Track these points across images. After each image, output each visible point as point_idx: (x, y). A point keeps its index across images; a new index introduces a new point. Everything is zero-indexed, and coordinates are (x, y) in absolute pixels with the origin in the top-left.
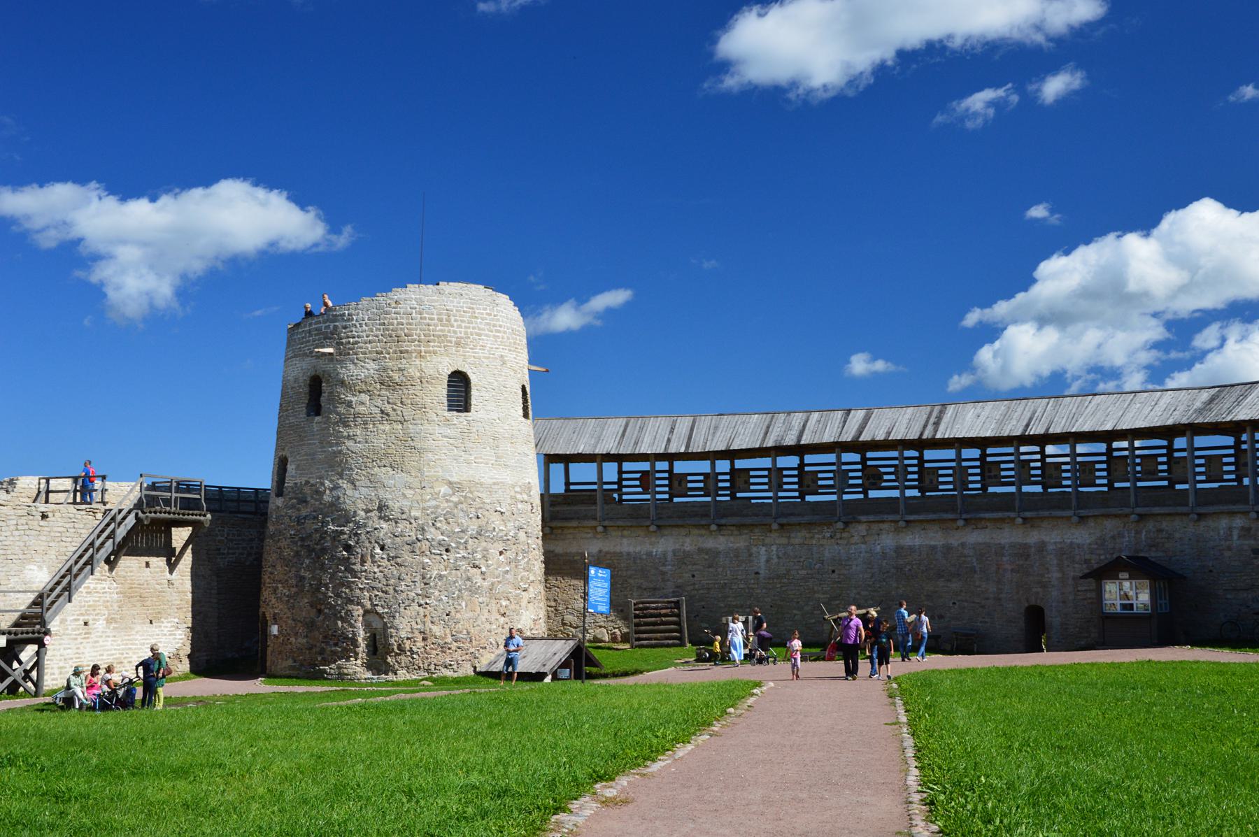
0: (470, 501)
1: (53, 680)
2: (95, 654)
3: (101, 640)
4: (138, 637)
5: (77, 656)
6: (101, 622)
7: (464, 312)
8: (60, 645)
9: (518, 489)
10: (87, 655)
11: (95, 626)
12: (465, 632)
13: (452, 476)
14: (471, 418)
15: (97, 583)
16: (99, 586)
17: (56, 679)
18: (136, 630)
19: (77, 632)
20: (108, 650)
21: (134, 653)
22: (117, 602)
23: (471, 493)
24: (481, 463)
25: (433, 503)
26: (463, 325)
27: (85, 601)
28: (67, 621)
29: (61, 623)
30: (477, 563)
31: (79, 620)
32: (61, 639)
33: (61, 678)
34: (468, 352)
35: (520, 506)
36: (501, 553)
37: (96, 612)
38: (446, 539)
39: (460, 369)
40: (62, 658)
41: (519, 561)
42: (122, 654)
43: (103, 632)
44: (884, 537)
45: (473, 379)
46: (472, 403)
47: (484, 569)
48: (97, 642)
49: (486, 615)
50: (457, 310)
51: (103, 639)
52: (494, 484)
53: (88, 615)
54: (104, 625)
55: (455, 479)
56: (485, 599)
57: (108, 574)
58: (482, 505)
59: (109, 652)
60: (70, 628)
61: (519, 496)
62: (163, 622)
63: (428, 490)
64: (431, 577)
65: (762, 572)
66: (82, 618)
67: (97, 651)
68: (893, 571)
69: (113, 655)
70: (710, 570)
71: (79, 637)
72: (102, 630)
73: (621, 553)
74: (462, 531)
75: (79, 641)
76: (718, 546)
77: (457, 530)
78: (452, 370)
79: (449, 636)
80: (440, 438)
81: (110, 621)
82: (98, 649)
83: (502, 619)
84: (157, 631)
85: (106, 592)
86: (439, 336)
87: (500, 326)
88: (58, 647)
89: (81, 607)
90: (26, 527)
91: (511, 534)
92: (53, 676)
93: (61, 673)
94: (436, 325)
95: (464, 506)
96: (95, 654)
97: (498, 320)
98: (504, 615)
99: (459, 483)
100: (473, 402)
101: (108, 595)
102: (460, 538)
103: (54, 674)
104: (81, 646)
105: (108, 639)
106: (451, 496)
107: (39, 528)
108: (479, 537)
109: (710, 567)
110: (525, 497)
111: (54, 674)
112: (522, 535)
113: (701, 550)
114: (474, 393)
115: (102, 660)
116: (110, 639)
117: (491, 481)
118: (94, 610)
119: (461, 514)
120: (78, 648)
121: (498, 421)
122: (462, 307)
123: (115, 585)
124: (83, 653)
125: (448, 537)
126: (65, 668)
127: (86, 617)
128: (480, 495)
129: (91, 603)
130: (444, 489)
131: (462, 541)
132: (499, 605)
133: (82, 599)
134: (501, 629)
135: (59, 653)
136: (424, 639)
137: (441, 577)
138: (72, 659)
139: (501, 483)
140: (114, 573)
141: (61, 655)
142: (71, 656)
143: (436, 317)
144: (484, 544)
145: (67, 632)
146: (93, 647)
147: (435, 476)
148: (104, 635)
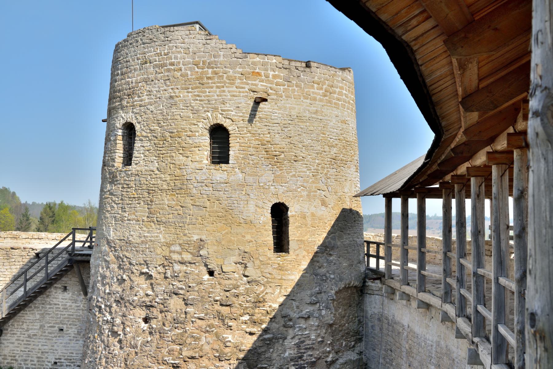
1: (32, 365)
5: (51, 351)
6: (73, 330)
8: (39, 342)
9: (173, 248)
10: (60, 351)
11: (67, 332)
13: (110, 236)
14: (130, 173)
15: (73, 303)
17: (35, 365)
19: (53, 335)
27: (61, 315)
28: (45, 327)
30: (115, 329)
31: (54, 327)
32: (39, 339)
33: (39, 365)
35: (177, 267)
37: (69, 323)
40: (41, 351)
43: (74, 337)
45: (138, 127)
46: (134, 155)
53: (62, 324)
60: (47, 331)
61: (176, 257)
66: (57, 326)
67: (68, 350)
71: (54, 339)
72: (74, 335)
77: (107, 291)
80: (108, 196)
82: (69, 349)
85: (80, 310)
87: (172, 64)
88: (37, 344)
89: (57, 318)
91: (157, 300)
92: (33, 363)
93: (38, 361)
104: (55, 345)
105: (77, 342)
110: (187, 257)
112: (175, 303)
115: (71, 356)
117: (139, 241)
118: (68, 321)
120: (53, 346)
121: (157, 172)
124: (56, 350)
126: (42, 358)
127: (61, 326)
128: (127, 254)
129: (66, 316)
135: (37, 348)
138: (47, 353)
139: (151, 241)
141: (39, 349)
142: (47, 351)
144: (124, 309)
145: (44, 334)
146: (65, 346)
148: (75, 339)
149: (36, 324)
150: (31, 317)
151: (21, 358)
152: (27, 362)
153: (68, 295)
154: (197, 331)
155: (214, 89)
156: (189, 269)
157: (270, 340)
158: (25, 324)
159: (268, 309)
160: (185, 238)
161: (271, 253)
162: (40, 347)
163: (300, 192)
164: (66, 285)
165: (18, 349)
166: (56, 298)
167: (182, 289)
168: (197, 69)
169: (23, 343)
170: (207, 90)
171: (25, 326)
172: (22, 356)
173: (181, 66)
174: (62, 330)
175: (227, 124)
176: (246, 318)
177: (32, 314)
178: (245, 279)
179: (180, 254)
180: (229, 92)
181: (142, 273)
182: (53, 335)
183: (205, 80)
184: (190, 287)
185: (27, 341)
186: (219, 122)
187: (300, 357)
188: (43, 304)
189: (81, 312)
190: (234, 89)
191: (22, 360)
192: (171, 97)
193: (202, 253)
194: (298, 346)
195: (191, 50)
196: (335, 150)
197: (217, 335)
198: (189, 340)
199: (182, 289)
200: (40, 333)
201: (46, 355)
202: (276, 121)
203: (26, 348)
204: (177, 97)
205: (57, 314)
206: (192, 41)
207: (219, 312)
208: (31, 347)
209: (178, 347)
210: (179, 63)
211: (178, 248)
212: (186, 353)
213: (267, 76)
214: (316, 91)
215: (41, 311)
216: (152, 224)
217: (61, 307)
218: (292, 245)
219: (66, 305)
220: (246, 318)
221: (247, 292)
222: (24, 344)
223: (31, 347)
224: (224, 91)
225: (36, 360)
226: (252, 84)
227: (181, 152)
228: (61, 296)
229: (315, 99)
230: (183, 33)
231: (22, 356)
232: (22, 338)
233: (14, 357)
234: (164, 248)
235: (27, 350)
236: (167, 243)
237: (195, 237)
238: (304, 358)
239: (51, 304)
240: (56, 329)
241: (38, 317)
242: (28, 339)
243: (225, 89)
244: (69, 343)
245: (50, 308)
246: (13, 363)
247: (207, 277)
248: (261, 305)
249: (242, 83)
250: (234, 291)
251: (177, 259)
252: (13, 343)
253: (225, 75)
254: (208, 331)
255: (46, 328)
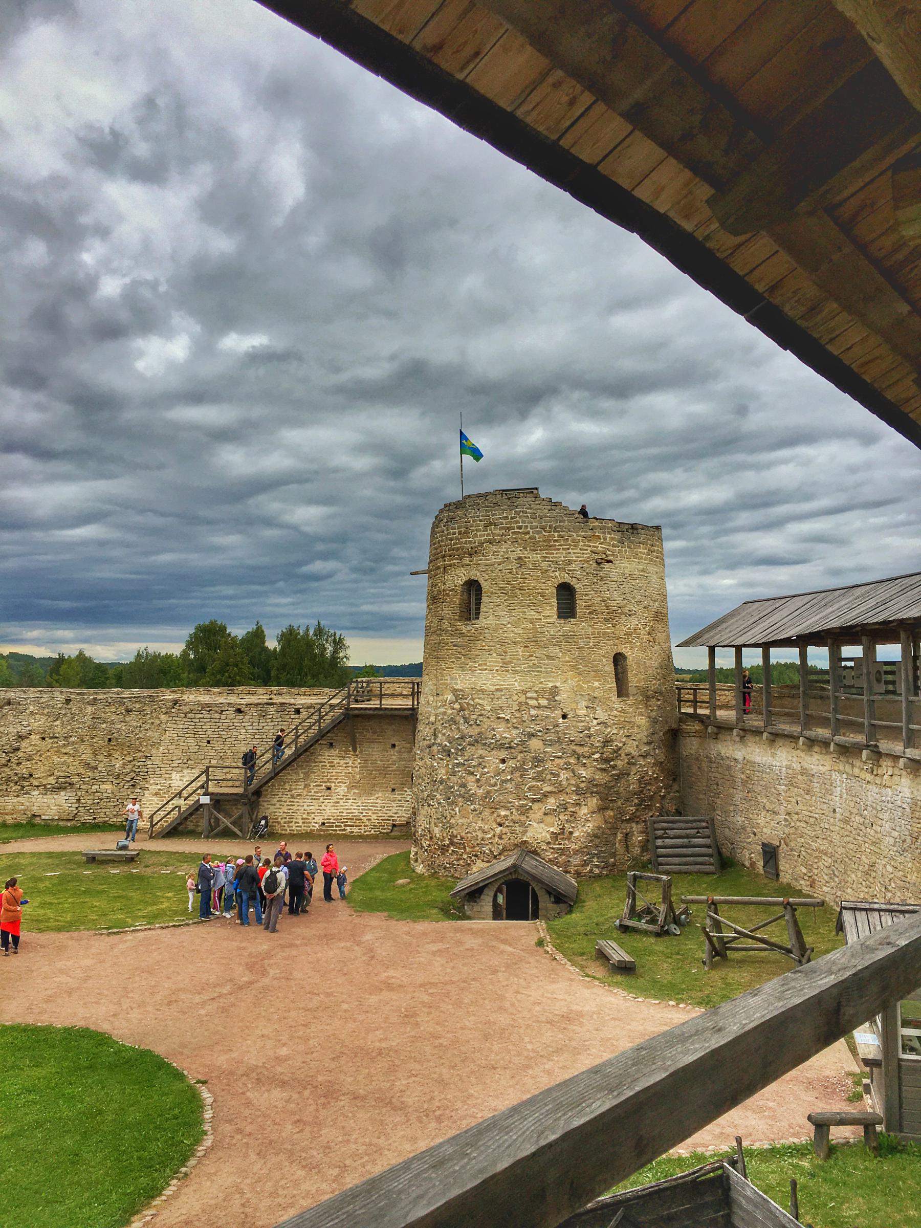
0: (472, 709)
2: (336, 811)
3: (341, 802)
4: (378, 801)
7: (480, 521)
9: (529, 695)
11: (336, 791)
12: (459, 837)
13: (456, 684)
16: (342, 762)
17: (300, 827)
18: (377, 796)
19: (320, 795)
20: (347, 809)
21: (373, 813)
22: (360, 773)
23: (473, 699)
24: (486, 669)
25: (442, 710)
26: (478, 533)
29: (305, 787)
30: (472, 769)
31: (321, 786)
34: (481, 560)
35: (533, 712)
36: (503, 761)
38: (448, 745)
39: (472, 578)
41: (527, 770)
42: (362, 813)
44: (903, 780)
45: (484, 585)
46: (481, 610)
47: (478, 777)
48: (338, 802)
49: (480, 824)
50: (473, 521)
51: (344, 800)
52: (497, 690)
53: (330, 782)
54: (346, 791)
55: (458, 687)
56: (477, 807)
57: (352, 753)
58: (483, 712)
59: (349, 811)
62: (406, 791)
63: (441, 698)
64: (436, 781)
65: (837, 810)
68: (909, 839)
69: (352, 813)
70: (808, 797)
73: (755, 763)
74: (462, 738)
75: (321, 799)
76: (812, 766)
78: (465, 579)
79: (447, 839)
81: (350, 788)
83: (498, 830)
84: (399, 797)
86: (458, 549)
87: (520, 528)
88: (302, 804)
89: (324, 776)
90: (280, 719)
91: (515, 742)
93: (303, 823)
94: (457, 539)
95: (466, 713)
96: (336, 811)
97: (517, 522)
98: (500, 825)
99: (461, 690)
100: (483, 609)
101: (350, 768)
102: (460, 745)
103: (298, 823)
104: (323, 805)
106: (454, 703)
107: (290, 720)
108: (476, 744)
109: (808, 792)
110: (544, 702)
111: (298, 823)
113: (804, 772)
114: (485, 600)
116: (350, 801)
117: (493, 688)
118: (336, 779)
119: (462, 721)
122: (478, 517)
123: (359, 761)
125: (450, 743)
127: (328, 784)
128: (481, 702)
129: (334, 774)
130: (450, 697)
131: (460, 748)
132: (495, 815)
133: (326, 771)
134: (497, 839)
135: (303, 808)
136: (431, 838)
137: (441, 782)
140: (357, 753)
143: (457, 531)
144: (480, 752)
145: (310, 794)
146: (334, 806)
147: (445, 684)
148: (345, 798)
149: (299, 783)
150: (294, 777)
151: (284, 820)
152: (291, 825)
153: (335, 752)
154: (556, 769)
155: (561, 551)
156: (546, 713)
157: (618, 775)
158: (287, 784)
159: (615, 748)
160: (540, 686)
161: (614, 698)
162: (305, 807)
163: (635, 643)
164: (332, 741)
165: (280, 811)
166: (321, 755)
167: (540, 731)
168: (544, 533)
169: (285, 804)
170: (555, 552)
171: (287, 786)
172: (285, 818)
173: (529, 529)
174: (329, 789)
175: (573, 582)
176: (597, 756)
177: (295, 773)
178: (595, 722)
179: (537, 699)
180: (574, 553)
181: (499, 718)
182: (320, 795)
183: (552, 543)
184: (547, 729)
185: (290, 802)
186: (566, 580)
187: (642, 791)
188: (307, 762)
189: (350, 768)
190: (578, 551)
191: (285, 823)
192: (520, 558)
193: (556, 698)
194: (639, 781)
195: (537, 515)
196: (657, 604)
197: (573, 771)
198: (549, 777)
199: (540, 731)
200: (305, 793)
201: (313, 815)
202: (613, 579)
203: (290, 809)
204: (526, 557)
205: (324, 772)
206: (538, 506)
207: (574, 751)
208: (295, 808)
209: (539, 784)
210: (526, 527)
211: (535, 695)
212: (547, 788)
213: (605, 539)
214: (642, 550)
215: (304, 769)
216: (507, 673)
217: (328, 765)
218: (632, 690)
219: (333, 762)
220: (597, 756)
221: (598, 733)
222: (288, 805)
223: (295, 808)
224: (570, 553)
225: (301, 821)
226: (594, 547)
227: (532, 608)
228: (327, 754)
229: (641, 558)
230: (530, 499)
231: (285, 818)
232: (284, 799)
233: (277, 819)
234: (520, 695)
235: (290, 811)
236: (523, 691)
237: (550, 685)
238: (644, 792)
239: (316, 762)
240: (323, 787)
241: (302, 776)
242: (292, 800)
243: (570, 551)
244: (338, 802)
245: (315, 766)
246: (275, 826)
247: (561, 720)
248: (609, 744)
249: (584, 545)
250: (586, 732)
251: (533, 705)
252: (274, 805)
253: (570, 538)
254: (566, 769)
255: (312, 787)
